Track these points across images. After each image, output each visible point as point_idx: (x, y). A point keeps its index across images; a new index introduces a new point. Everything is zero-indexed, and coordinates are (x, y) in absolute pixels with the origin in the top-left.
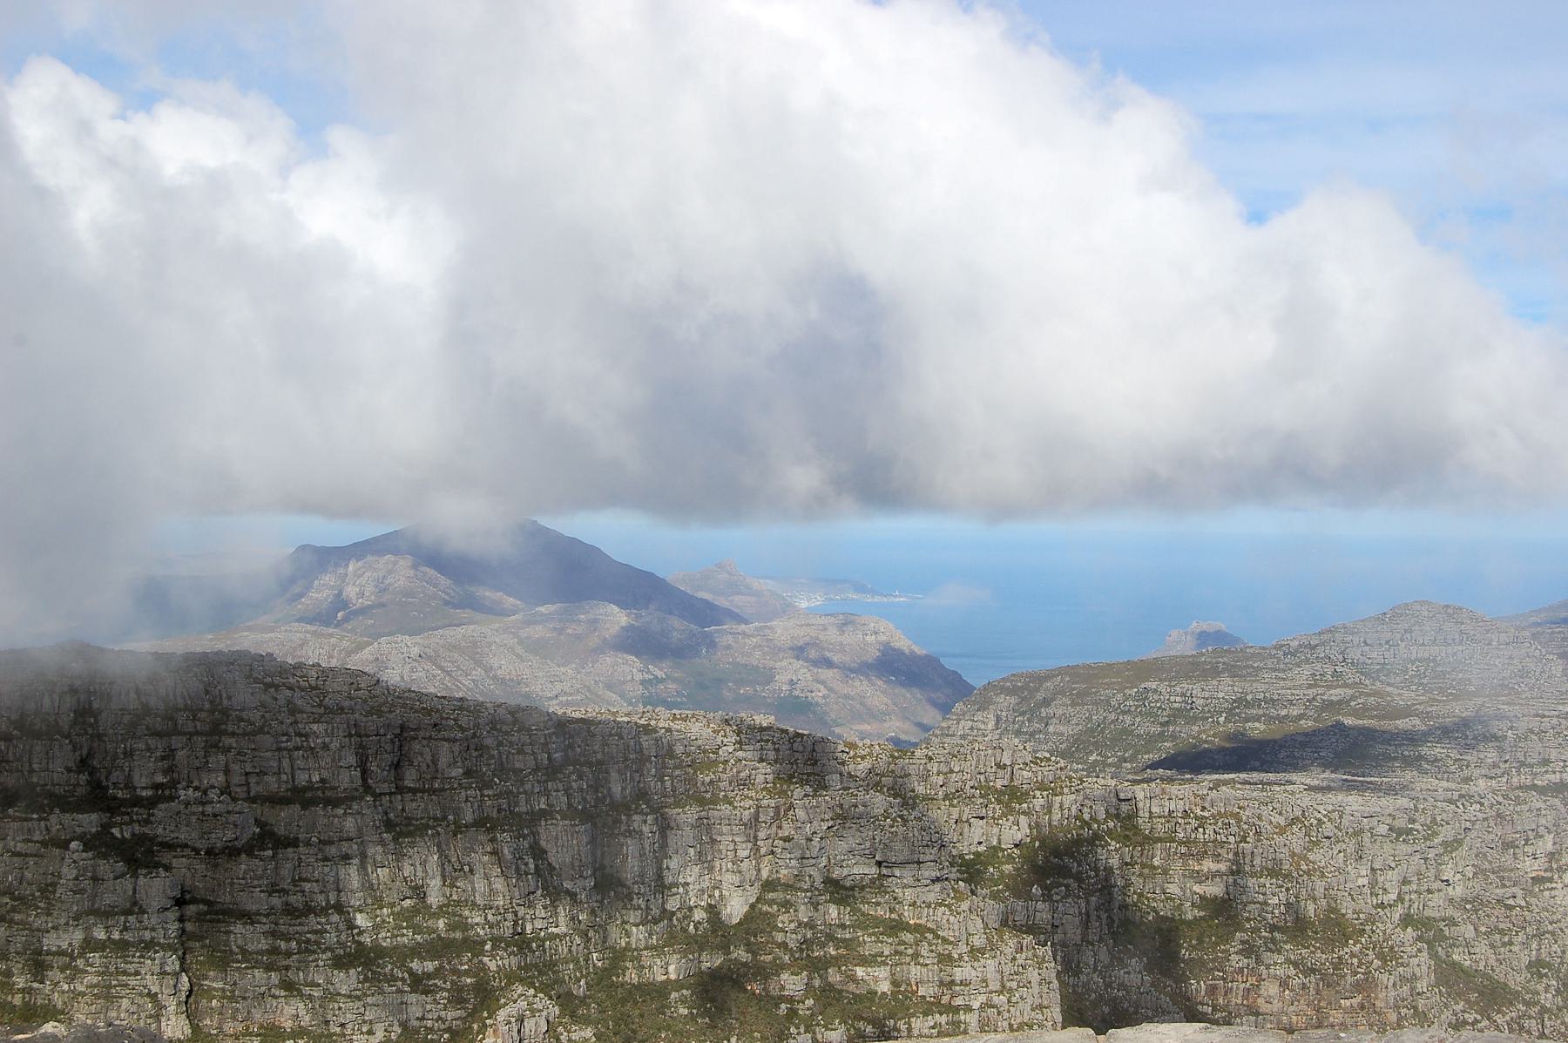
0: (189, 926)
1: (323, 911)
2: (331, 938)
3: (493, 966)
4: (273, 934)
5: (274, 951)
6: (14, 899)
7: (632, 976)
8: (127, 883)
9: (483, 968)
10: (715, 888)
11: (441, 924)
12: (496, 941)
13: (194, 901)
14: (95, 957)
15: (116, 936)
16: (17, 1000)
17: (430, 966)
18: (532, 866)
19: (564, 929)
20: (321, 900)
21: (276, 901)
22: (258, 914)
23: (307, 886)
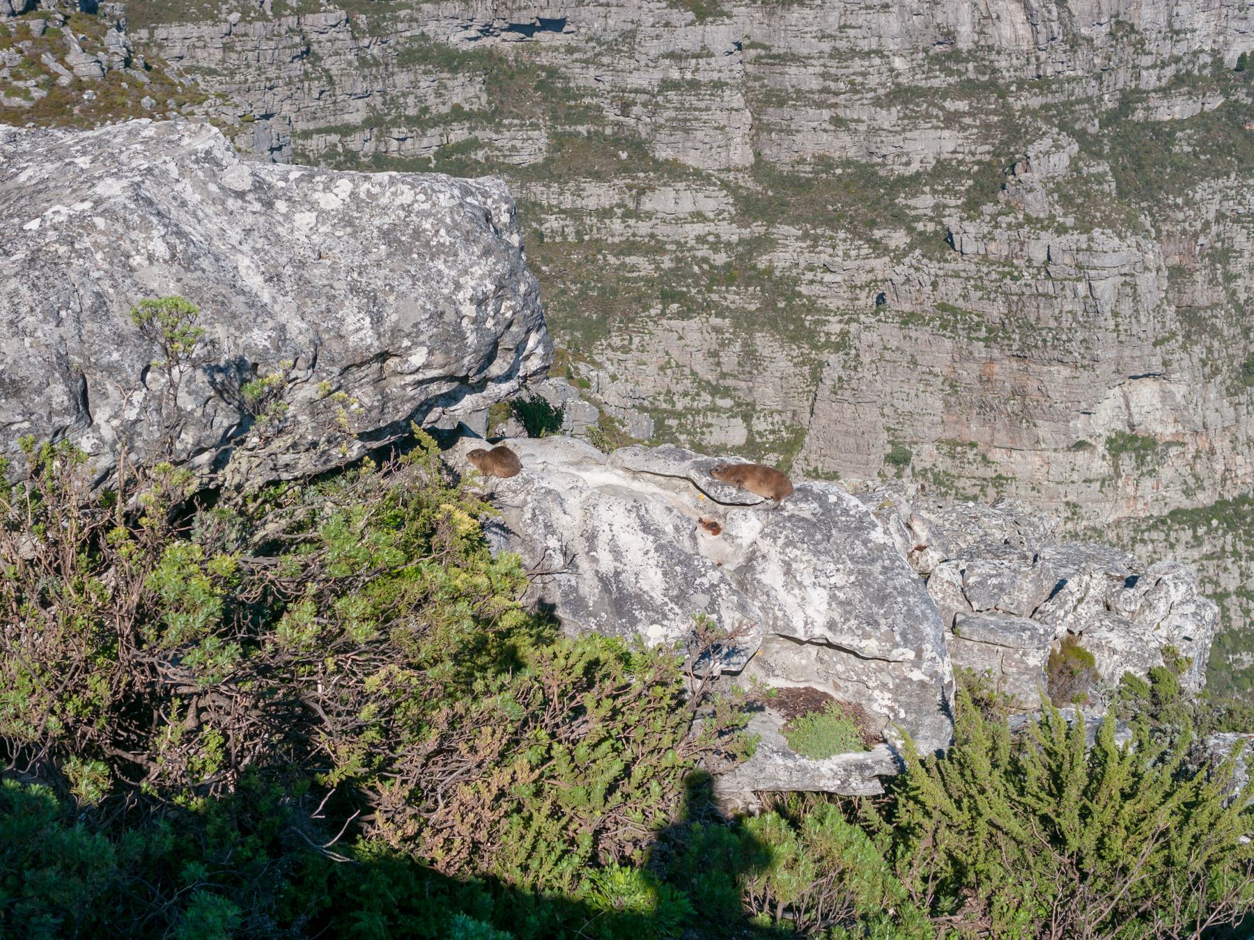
0: (750, 68)
1: (868, 55)
2: (873, 81)
3: (1018, 106)
4: (824, 76)
5: (825, 90)
6: (600, 43)
7: (1139, 115)
8: (699, 29)
9: (1006, 106)
10: (1219, 34)
11: (971, 66)
12: (1021, 84)
13: (753, 45)
14: (671, 94)
15: (688, 76)
16: (608, 131)
17: (963, 105)
18: (1055, 14)
19: (1080, 73)
20: (864, 45)
21: (826, 46)
22: (809, 57)
23: (851, 32)
